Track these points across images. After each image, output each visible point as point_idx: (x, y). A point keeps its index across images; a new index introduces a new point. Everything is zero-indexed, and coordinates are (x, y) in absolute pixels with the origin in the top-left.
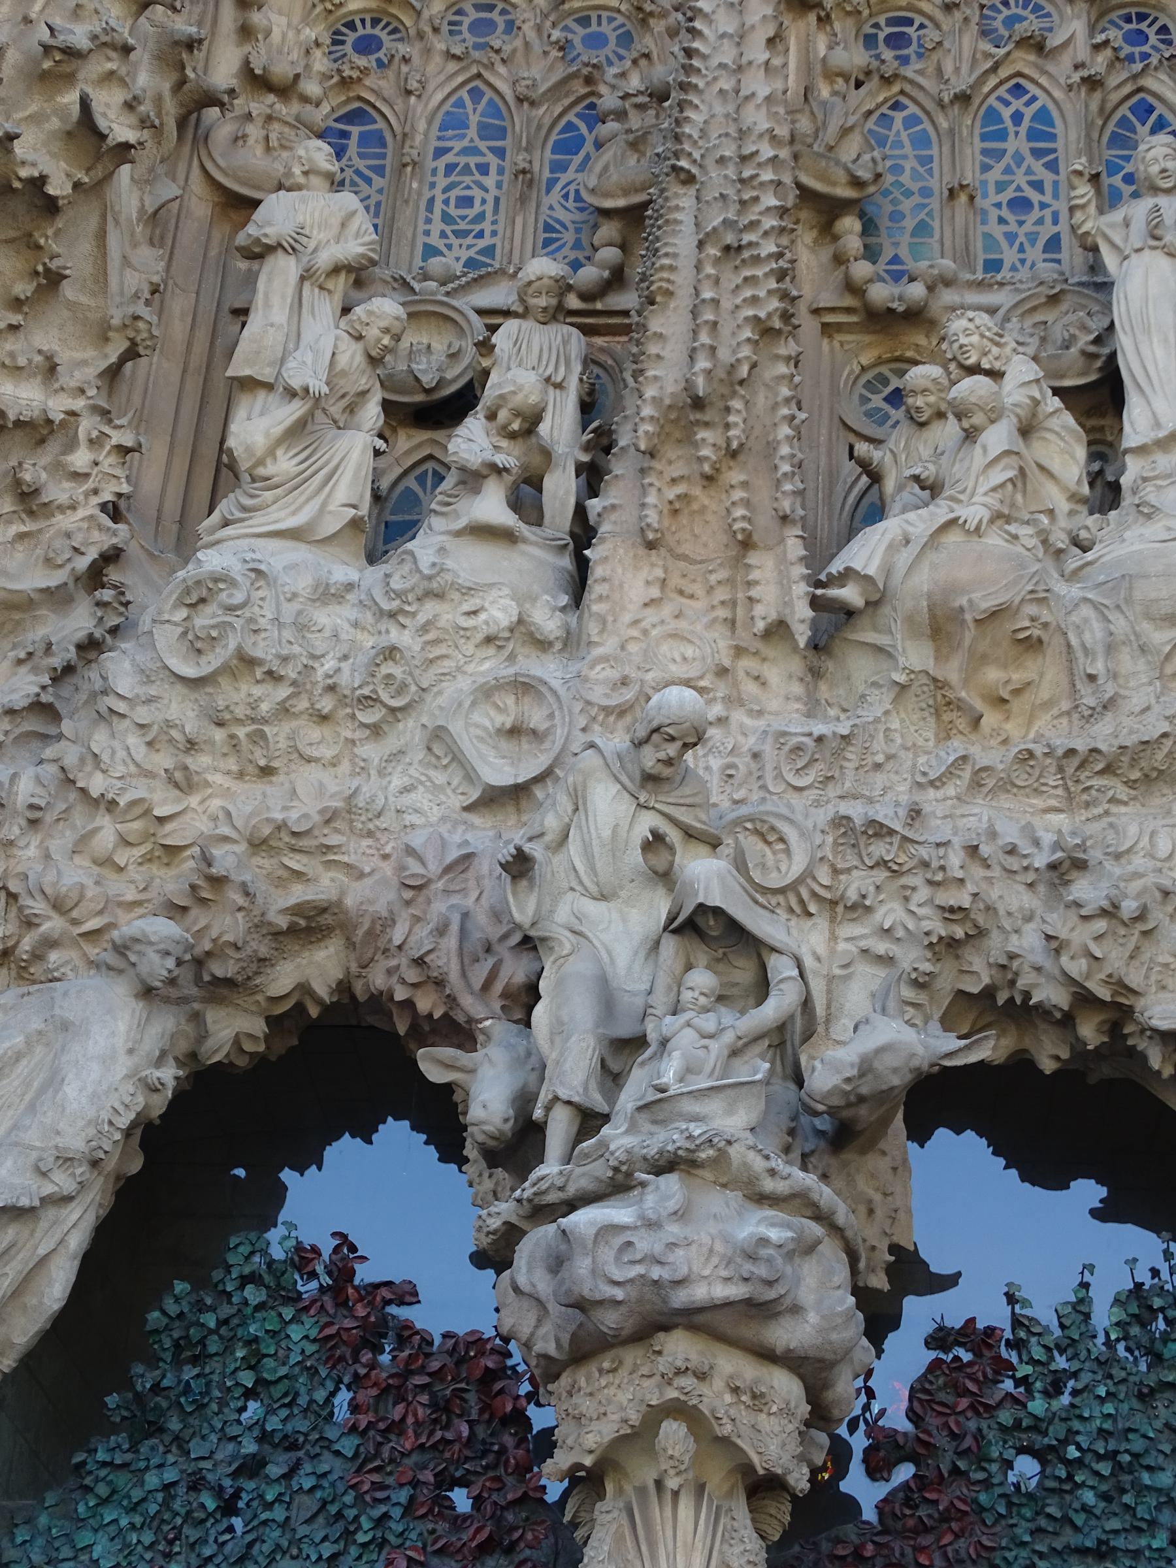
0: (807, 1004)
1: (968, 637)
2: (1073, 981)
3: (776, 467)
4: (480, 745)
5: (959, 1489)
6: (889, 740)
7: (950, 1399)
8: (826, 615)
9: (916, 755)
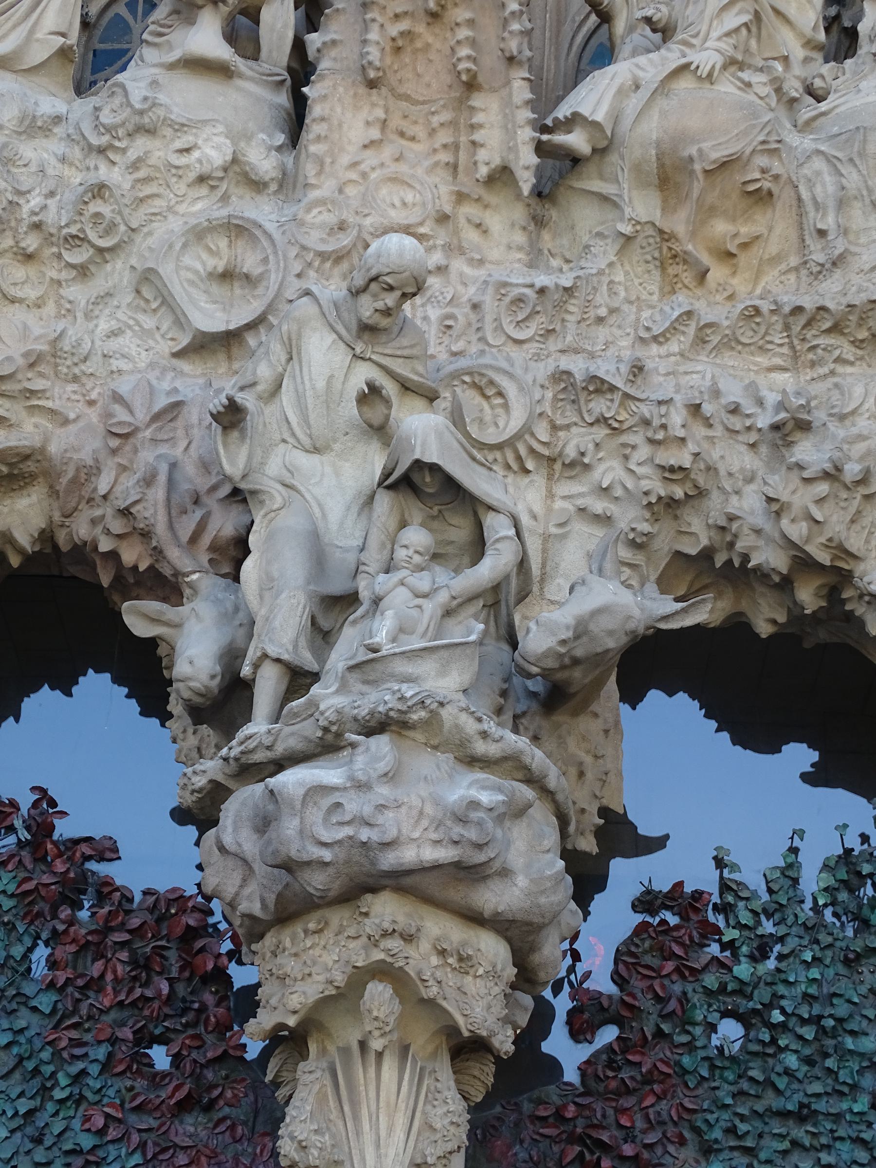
0: (523, 564)
1: (697, 187)
2: (791, 544)
4: (191, 290)
5: (662, 1051)
6: (612, 293)
7: (655, 962)
8: (550, 162)
9: (640, 310)
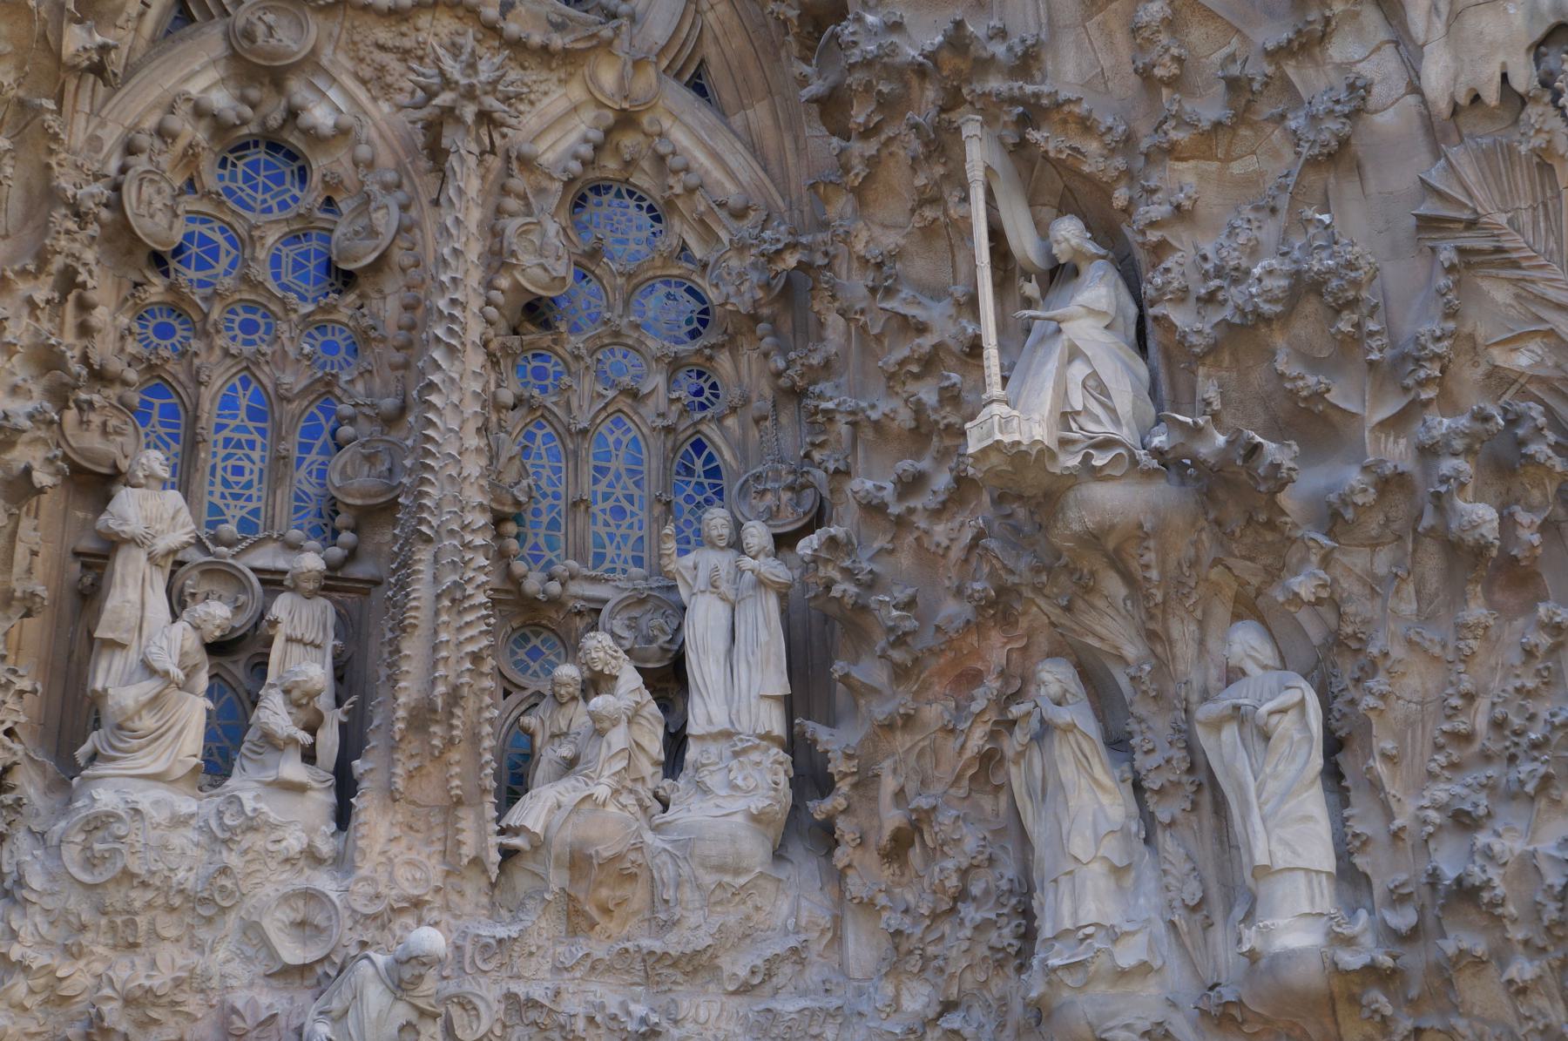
1: (595, 872)
3: (480, 755)
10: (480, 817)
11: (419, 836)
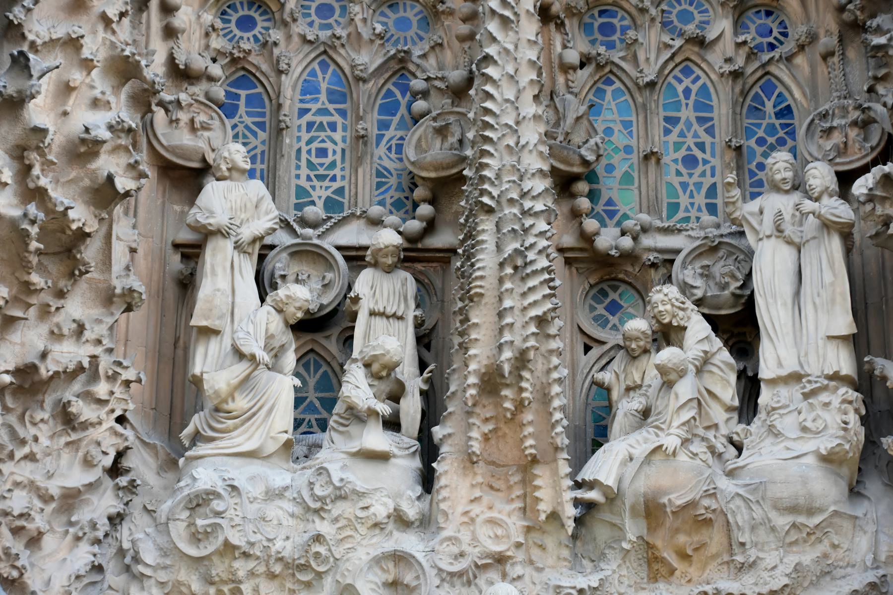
1: (669, 521)
3: (551, 414)
10: (555, 472)
11: (500, 494)
